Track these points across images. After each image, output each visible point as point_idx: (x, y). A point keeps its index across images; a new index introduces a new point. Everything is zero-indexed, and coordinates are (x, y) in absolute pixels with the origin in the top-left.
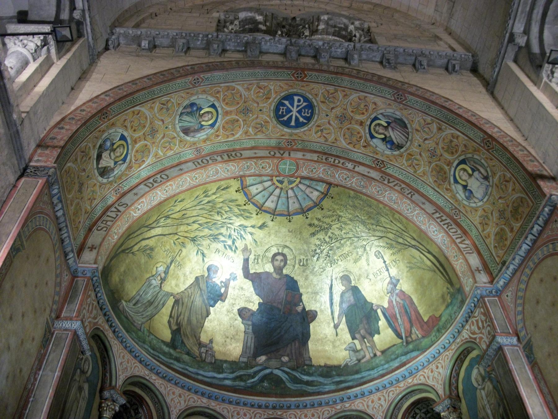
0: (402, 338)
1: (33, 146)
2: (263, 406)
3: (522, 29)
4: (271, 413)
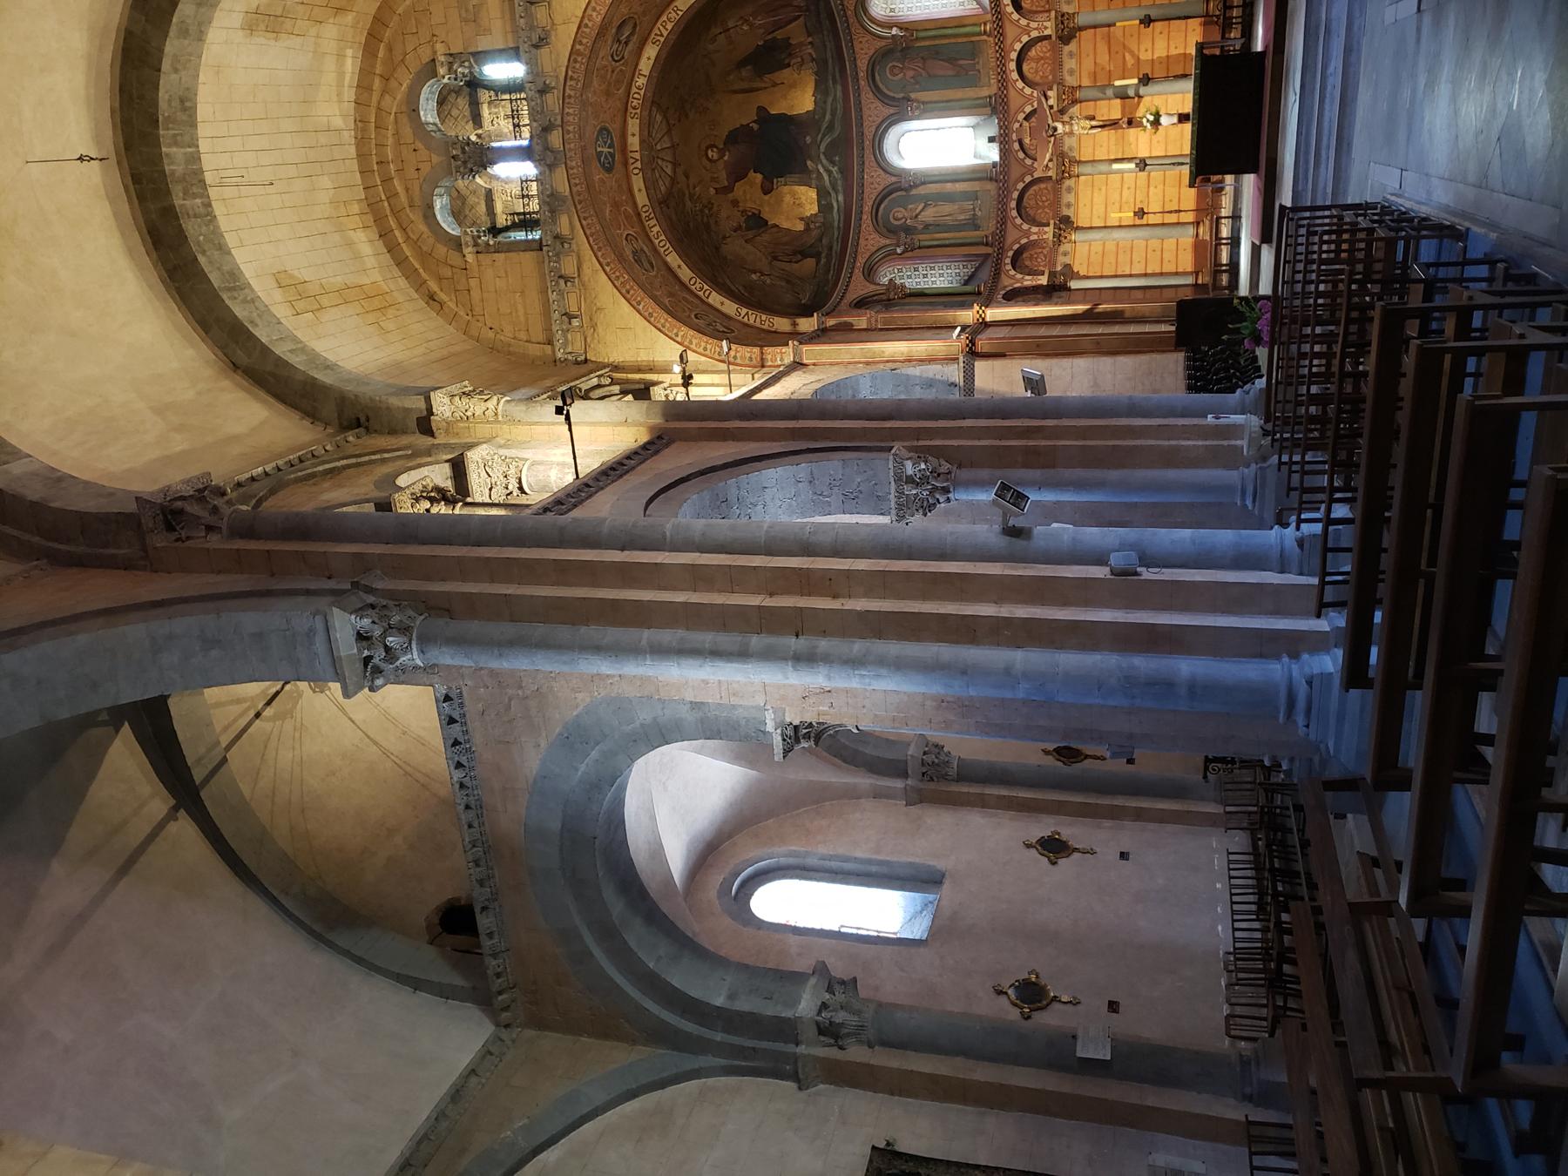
0: (799, 17)
1: (765, 370)
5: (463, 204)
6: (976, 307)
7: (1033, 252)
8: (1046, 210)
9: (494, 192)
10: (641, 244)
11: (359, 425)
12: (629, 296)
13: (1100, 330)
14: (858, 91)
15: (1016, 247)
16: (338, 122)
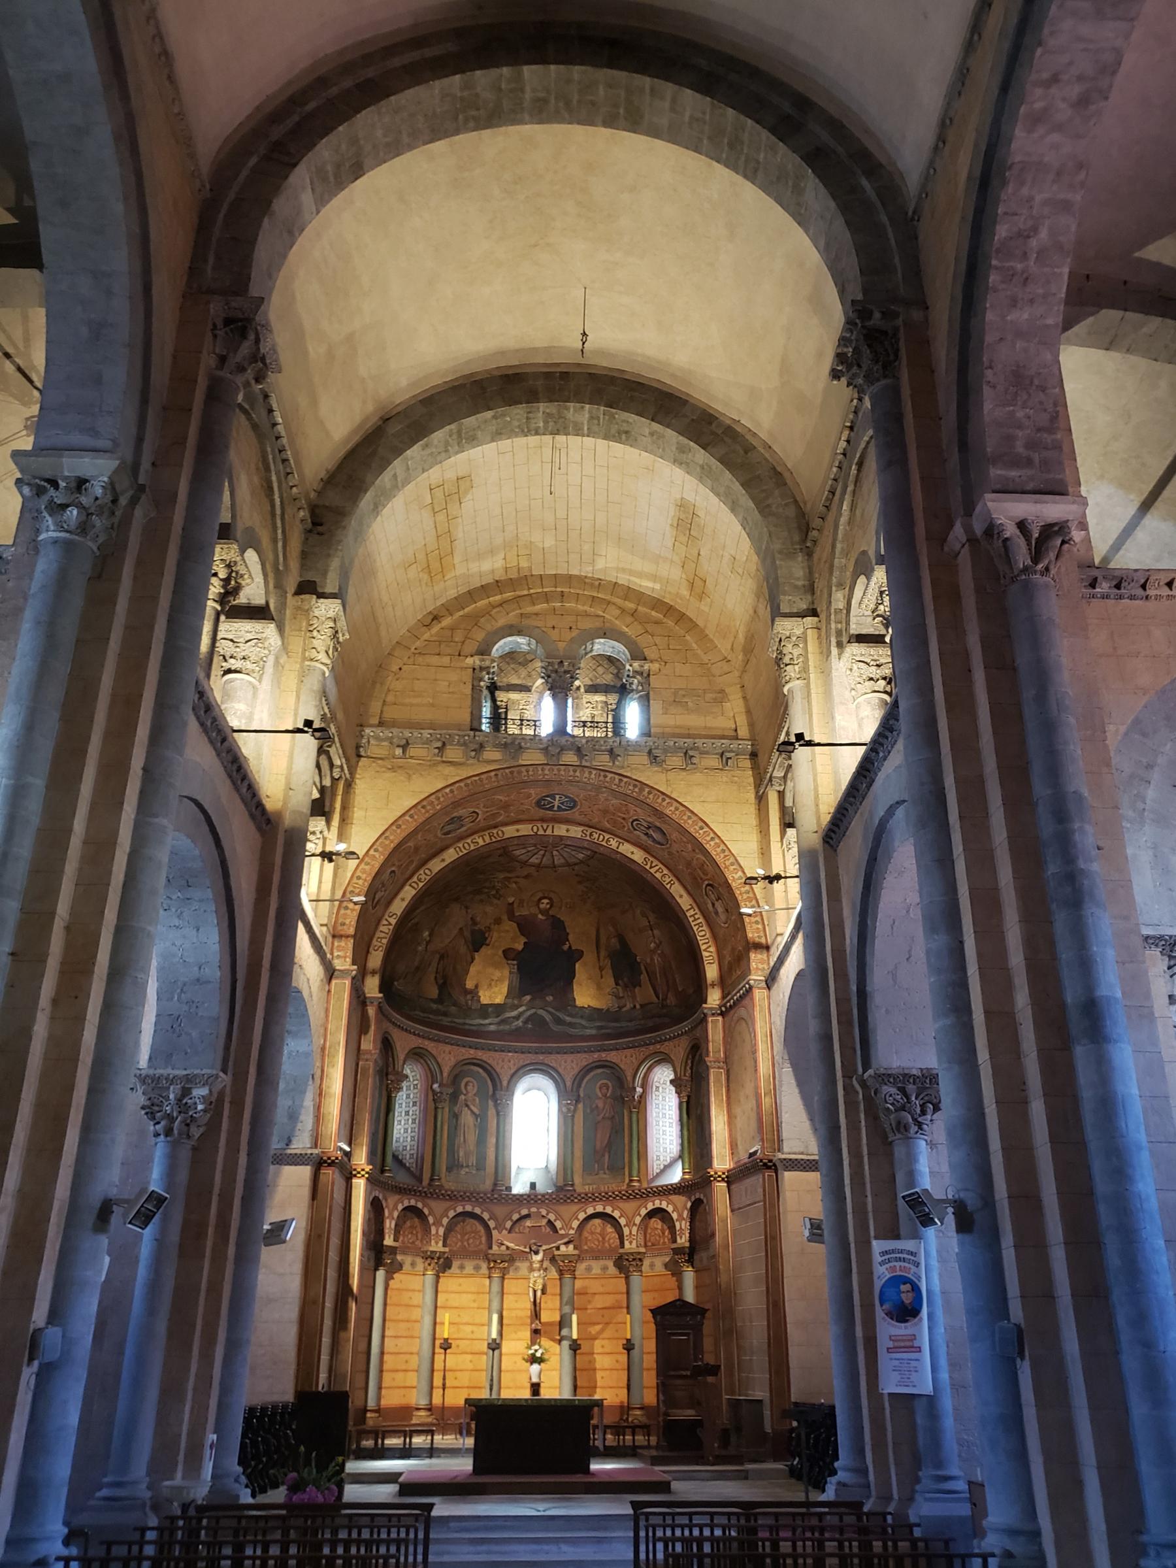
1: (330, 939)
3: (783, 774)
5: (520, 663)
6: (368, 1168)
7: (419, 1229)
8: (459, 1244)
9: (528, 694)
10: (468, 826)
11: (314, 524)
12: (419, 807)
13: (329, 1305)
14: (589, 1051)
15: (426, 1211)
16: (600, 564)
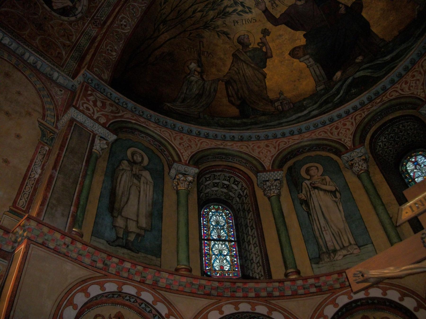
2: (359, 106)
4: (369, 106)
